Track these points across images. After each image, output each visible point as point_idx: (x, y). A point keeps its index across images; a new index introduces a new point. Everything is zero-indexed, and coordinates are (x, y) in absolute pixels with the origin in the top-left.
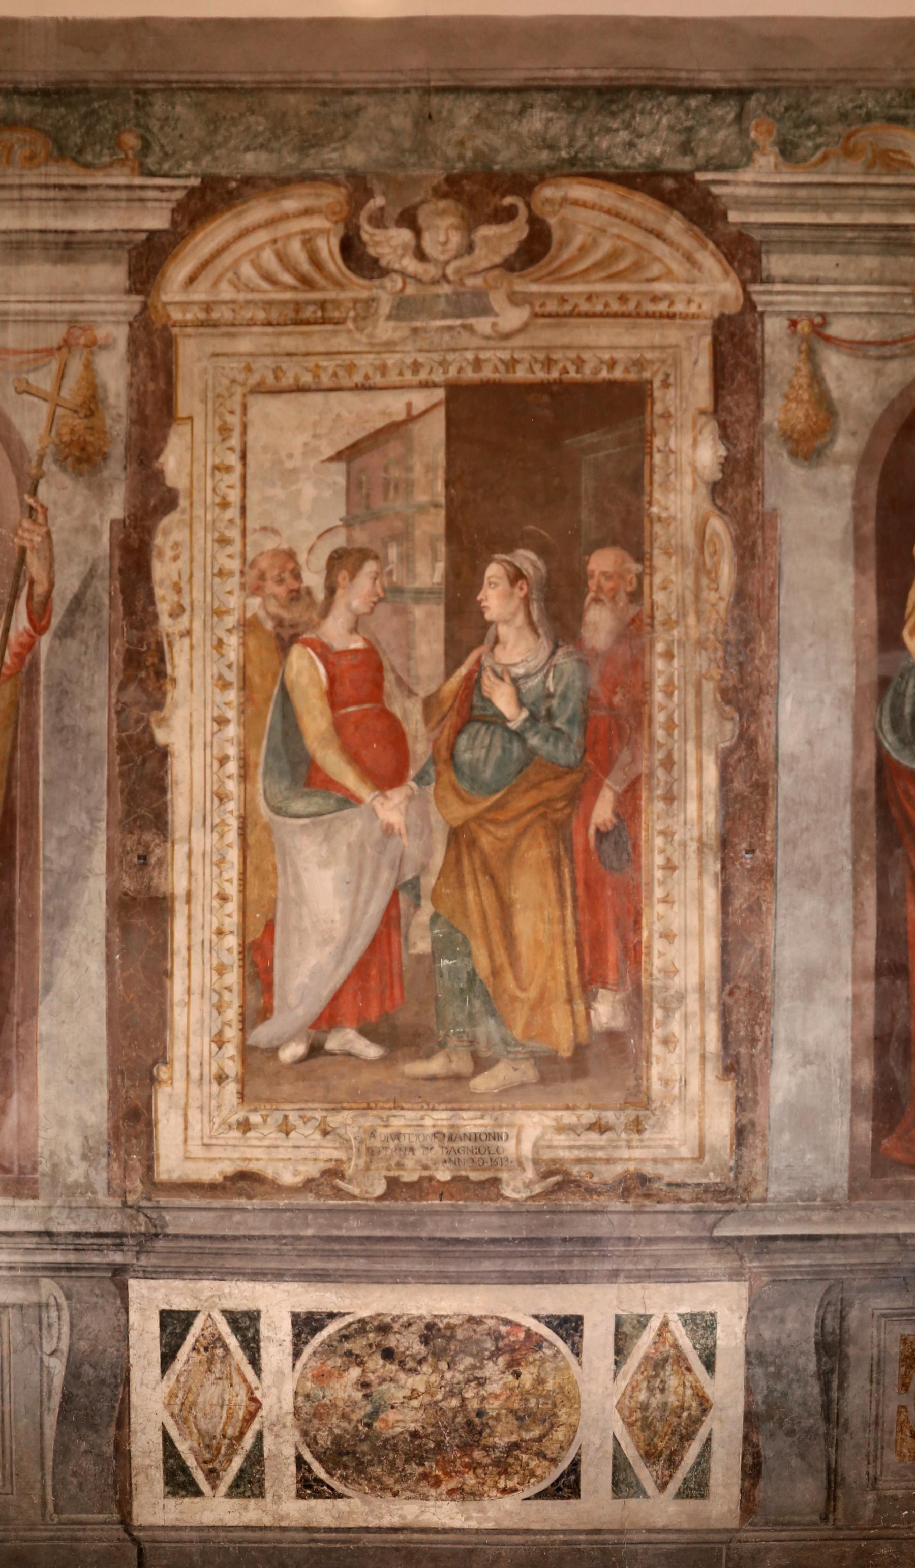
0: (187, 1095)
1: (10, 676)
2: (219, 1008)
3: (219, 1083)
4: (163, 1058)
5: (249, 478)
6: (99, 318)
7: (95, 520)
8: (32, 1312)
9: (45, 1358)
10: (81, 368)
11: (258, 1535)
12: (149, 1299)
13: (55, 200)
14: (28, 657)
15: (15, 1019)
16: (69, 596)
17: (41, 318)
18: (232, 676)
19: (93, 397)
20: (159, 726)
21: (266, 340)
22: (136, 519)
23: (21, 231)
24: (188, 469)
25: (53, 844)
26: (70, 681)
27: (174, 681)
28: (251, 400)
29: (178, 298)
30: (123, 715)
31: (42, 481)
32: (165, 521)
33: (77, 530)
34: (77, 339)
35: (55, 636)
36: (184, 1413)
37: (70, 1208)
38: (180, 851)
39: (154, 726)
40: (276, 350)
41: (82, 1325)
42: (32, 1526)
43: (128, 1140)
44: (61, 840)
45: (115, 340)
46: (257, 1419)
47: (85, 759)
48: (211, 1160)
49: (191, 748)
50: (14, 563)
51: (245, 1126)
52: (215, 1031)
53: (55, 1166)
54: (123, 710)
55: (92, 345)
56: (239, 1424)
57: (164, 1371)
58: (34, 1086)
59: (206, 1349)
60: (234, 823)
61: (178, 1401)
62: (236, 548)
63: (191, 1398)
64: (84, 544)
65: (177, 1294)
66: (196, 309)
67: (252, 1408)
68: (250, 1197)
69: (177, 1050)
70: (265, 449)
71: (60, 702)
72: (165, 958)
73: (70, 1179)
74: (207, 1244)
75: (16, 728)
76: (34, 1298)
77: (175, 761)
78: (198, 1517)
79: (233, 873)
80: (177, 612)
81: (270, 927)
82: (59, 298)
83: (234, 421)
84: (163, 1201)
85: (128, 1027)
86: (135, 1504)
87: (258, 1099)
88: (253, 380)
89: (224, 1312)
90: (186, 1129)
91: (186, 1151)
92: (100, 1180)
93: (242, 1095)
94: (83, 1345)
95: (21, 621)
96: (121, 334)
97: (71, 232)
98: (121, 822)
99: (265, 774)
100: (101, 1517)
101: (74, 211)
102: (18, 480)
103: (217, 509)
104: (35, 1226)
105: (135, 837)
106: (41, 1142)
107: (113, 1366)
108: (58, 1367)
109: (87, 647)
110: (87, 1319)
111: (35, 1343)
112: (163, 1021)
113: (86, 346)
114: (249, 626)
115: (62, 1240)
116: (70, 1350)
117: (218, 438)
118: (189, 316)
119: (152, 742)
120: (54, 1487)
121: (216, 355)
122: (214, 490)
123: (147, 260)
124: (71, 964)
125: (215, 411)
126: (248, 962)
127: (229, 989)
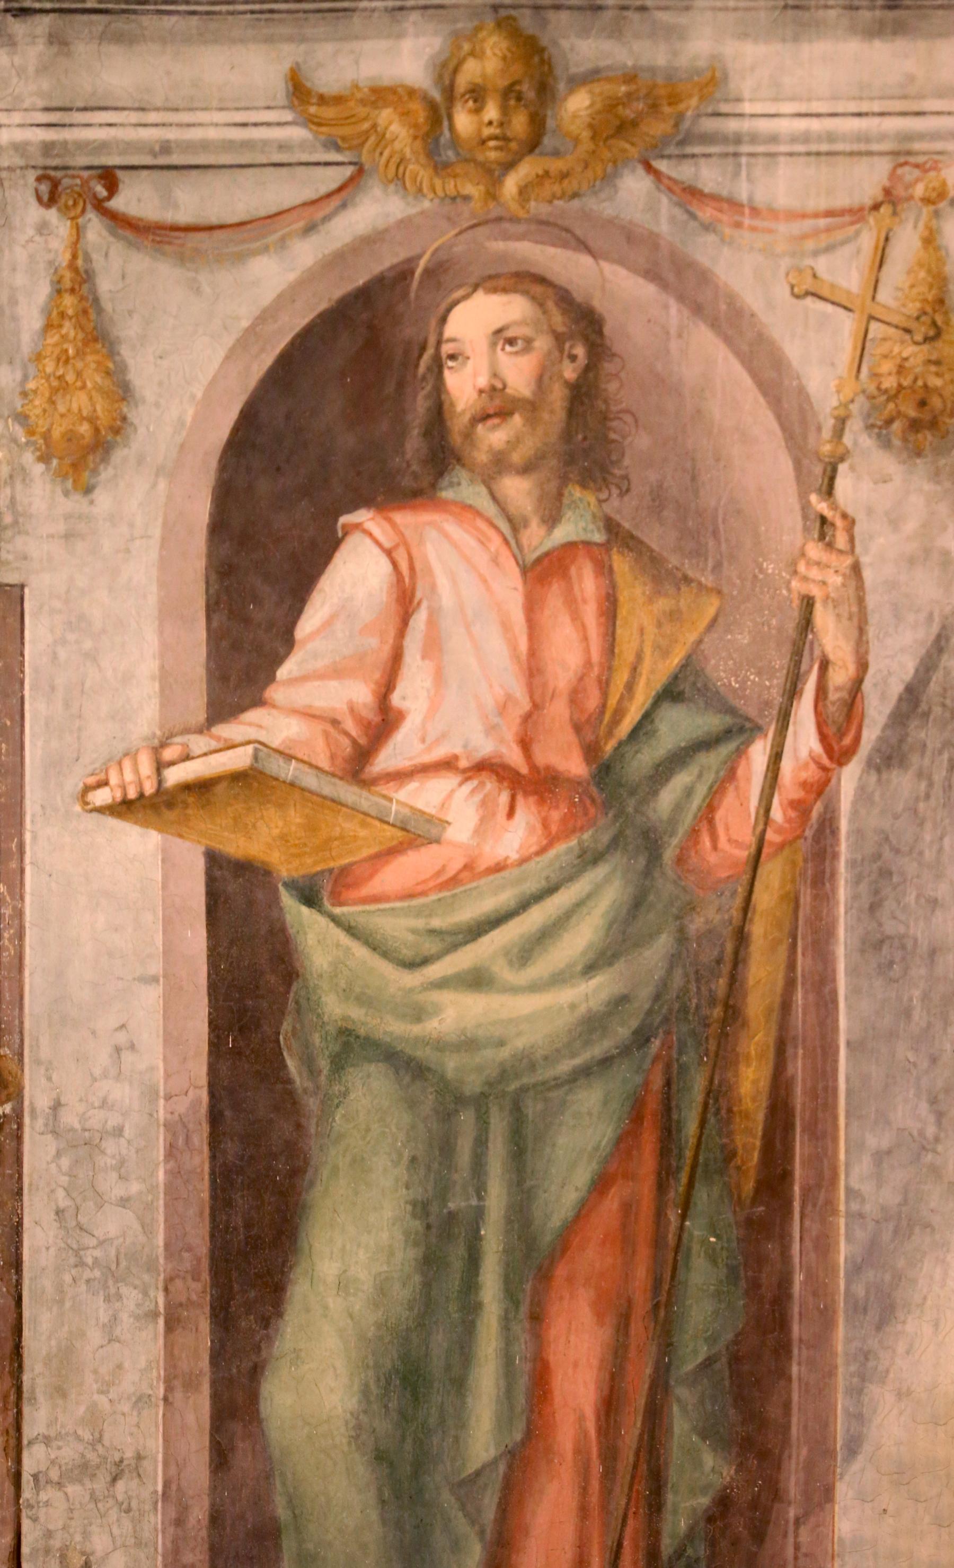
1: (781, 846)
10: (917, 243)
14: (817, 810)
16: (896, 689)
17: (839, 147)
19: (941, 301)
26: (897, 851)
31: (842, 468)
33: (912, 561)
35: (870, 764)
47: (925, 997)
50: (791, 627)
71: (877, 892)
82: (876, 107)
95: (804, 738)
109: (931, 785)
113: (927, 201)
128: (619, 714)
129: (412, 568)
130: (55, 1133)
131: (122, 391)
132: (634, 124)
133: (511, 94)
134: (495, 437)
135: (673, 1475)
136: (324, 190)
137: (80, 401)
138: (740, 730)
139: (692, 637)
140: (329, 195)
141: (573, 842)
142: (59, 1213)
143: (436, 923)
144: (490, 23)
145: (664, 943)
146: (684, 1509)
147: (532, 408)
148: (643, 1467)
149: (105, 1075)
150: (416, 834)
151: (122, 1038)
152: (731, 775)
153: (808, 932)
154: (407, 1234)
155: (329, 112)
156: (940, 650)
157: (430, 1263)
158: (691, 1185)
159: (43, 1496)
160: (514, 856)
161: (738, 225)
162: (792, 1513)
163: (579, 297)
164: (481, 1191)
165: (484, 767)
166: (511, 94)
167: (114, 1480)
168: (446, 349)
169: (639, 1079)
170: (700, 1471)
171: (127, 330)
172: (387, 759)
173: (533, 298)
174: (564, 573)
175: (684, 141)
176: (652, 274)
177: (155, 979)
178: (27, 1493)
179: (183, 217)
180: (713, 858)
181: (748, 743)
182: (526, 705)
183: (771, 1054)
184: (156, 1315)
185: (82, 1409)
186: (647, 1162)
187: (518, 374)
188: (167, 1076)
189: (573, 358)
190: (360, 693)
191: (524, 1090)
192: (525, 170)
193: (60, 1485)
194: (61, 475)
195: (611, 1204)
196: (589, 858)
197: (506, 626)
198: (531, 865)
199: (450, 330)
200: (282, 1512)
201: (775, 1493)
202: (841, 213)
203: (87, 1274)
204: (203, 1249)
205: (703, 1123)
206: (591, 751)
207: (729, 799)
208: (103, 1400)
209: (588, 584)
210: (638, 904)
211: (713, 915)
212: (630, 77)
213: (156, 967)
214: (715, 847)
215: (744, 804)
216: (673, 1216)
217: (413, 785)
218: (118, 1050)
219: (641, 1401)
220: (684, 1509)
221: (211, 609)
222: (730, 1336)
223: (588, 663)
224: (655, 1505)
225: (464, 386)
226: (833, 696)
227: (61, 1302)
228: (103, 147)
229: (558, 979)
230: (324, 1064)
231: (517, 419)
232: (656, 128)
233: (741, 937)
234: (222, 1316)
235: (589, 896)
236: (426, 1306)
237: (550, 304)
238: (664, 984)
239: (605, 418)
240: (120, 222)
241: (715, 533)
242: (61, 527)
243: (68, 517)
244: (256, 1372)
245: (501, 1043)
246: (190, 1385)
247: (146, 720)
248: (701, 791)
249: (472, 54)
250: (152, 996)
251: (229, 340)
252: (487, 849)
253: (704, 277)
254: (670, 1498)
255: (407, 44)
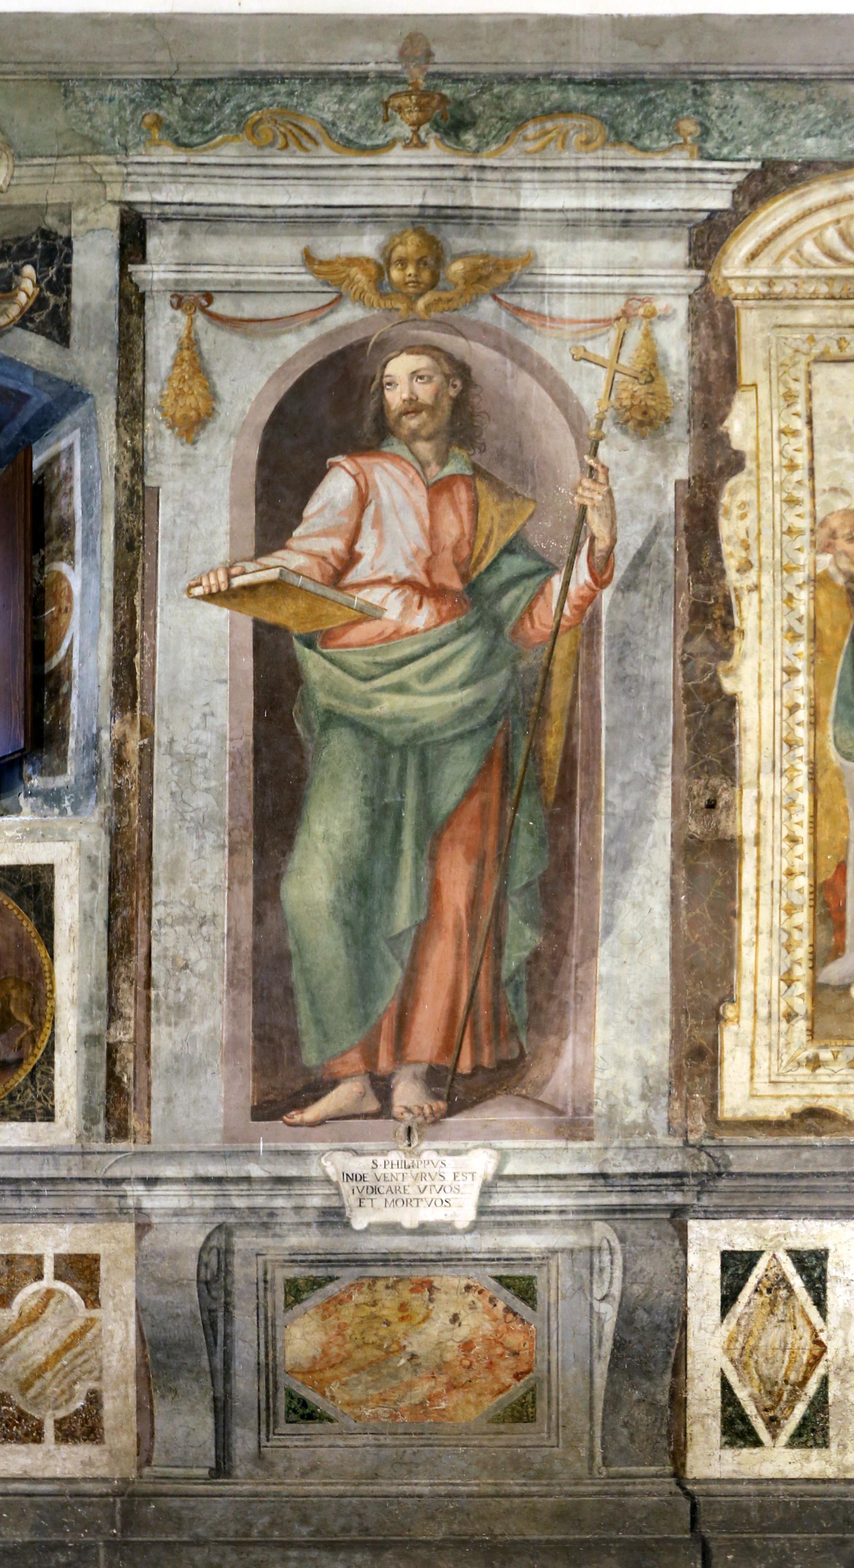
0: (754, 1033)
1: (570, 628)
2: (788, 947)
3: (788, 1021)
4: (730, 998)
5: (816, 441)
6: (658, 291)
7: (660, 480)
8: (584, 1257)
9: (596, 1304)
11: (821, 1488)
12: (709, 1241)
13: (612, 181)
14: (589, 610)
15: (574, 962)
16: (632, 552)
18: (802, 629)
19: (654, 365)
20: (727, 676)
21: (829, 312)
22: (702, 479)
23: (578, 210)
24: (753, 433)
25: (615, 790)
26: (633, 633)
27: (742, 632)
28: (815, 368)
29: (739, 273)
30: (689, 665)
31: (601, 443)
32: (732, 482)
33: (640, 490)
34: (635, 309)
35: (618, 589)
36: (745, 1358)
37: (628, 1148)
38: (749, 795)
39: (721, 676)
40: (840, 322)
41: (636, 1268)
42: (577, 1480)
43: (691, 1079)
44: (624, 786)
45: (675, 311)
46: (822, 1363)
47: (649, 707)
48: (779, 1097)
49: (760, 697)
50: (574, 520)
51: (815, 1063)
52: (784, 969)
53: (611, 1107)
54: (689, 660)
55: (651, 316)
56: (803, 1369)
57: (724, 1314)
58: (592, 1027)
59: (769, 1291)
60: (803, 768)
61: (738, 1346)
62: (806, 508)
63: (752, 1342)
64: (648, 503)
65: (740, 1235)
66: (757, 283)
67: (816, 1352)
68: (818, 1134)
69: (745, 989)
70: (831, 415)
72: (733, 899)
73: (628, 1120)
74: (773, 1183)
75: (576, 678)
76: (586, 1242)
77: (743, 709)
78: (756, 1469)
79: (804, 817)
80: (745, 567)
81: (841, 867)
82: (617, 272)
83: (799, 388)
84: (727, 1139)
85: (692, 967)
86: (690, 1455)
87: (829, 1036)
88: (816, 351)
89: (789, 1252)
90: (752, 1067)
91: (752, 1089)
92: (660, 1120)
93: (811, 1032)
94: (637, 1290)
95: (582, 574)
96: (681, 306)
97: (629, 211)
98: (686, 767)
99: (835, 722)
100: (653, 1469)
101: (632, 191)
102: (577, 441)
103: (784, 471)
104: (589, 1169)
105: (702, 782)
106: (597, 1083)
107: (669, 1310)
108: (609, 1312)
109: (652, 600)
110: (642, 1262)
111: (584, 1288)
112: (729, 959)
113: (645, 316)
114: (818, 581)
115: (618, 1182)
116: (623, 1295)
117: (783, 404)
118: (750, 290)
119: (720, 691)
120: (603, 1438)
121: (780, 326)
122: (781, 453)
123: (708, 238)
124: (634, 905)
125: (779, 379)
126: (819, 901)
127: (799, 928)
128: (480, 559)
129: (367, 484)
130: (171, 755)
131: (212, 396)
132: (487, 277)
133: (420, 262)
134: (413, 423)
135: (508, 940)
136: (321, 304)
137: (190, 400)
138: (547, 569)
139: (520, 523)
140: (324, 307)
141: (455, 622)
142: (172, 794)
143: (379, 659)
144: (410, 229)
145: (504, 674)
146: (514, 958)
147: (432, 409)
148: (492, 936)
149: (198, 727)
150: (368, 614)
151: (207, 710)
152: (541, 591)
153: (584, 671)
154: (361, 813)
155: (324, 269)
156: (656, 534)
157: (375, 828)
158: (519, 795)
159: (163, 931)
160: (422, 627)
161: (543, 326)
162: (574, 962)
163: (458, 358)
164: (402, 794)
165: (404, 583)
166: (420, 262)
167: (201, 925)
168: (386, 380)
169: (491, 741)
170: (522, 940)
171: (216, 367)
172: (352, 577)
173: (433, 357)
174: (450, 490)
175: (514, 286)
176: (497, 348)
177: (225, 681)
178: (154, 928)
179: (246, 316)
180: (531, 632)
181: (551, 576)
182: (428, 553)
183: (564, 731)
184: (224, 847)
185: (183, 891)
186: (495, 782)
187: (425, 393)
188: (231, 729)
189: (455, 386)
190: (338, 544)
191: (426, 744)
192: (428, 297)
193: (172, 926)
194: (180, 435)
195: (475, 803)
196: (463, 630)
197: (418, 514)
198: (432, 632)
199: (389, 370)
200: (292, 948)
201: (565, 951)
202: (599, 321)
203: (187, 824)
204: (250, 816)
205: (526, 765)
206: (464, 577)
207: (541, 604)
208: (195, 886)
209: (462, 494)
210: (490, 653)
211: (532, 660)
212: (485, 256)
213: (226, 675)
214: (533, 627)
215: (548, 606)
216: (509, 811)
217: (367, 591)
218: (205, 715)
219: (491, 903)
220: (514, 958)
221: (258, 501)
222: (540, 872)
223: (463, 534)
224: (498, 954)
225: (395, 398)
226: (597, 554)
227: (173, 838)
228: (205, 282)
229: (446, 690)
230: (316, 727)
231: (424, 414)
232: (500, 280)
233: (547, 672)
234: (260, 849)
235: (463, 649)
236: (372, 849)
237: (442, 360)
238: (505, 694)
239: (472, 415)
240: (214, 318)
241: (532, 472)
242: (180, 460)
243: (183, 455)
244: (278, 878)
245: (414, 720)
246: (242, 881)
247: (222, 554)
248: (525, 598)
249: (401, 243)
250: (223, 690)
251: (270, 373)
252: (407, 623)
253: (526, 350)
254: (506, 951)
255: (366, 239)
